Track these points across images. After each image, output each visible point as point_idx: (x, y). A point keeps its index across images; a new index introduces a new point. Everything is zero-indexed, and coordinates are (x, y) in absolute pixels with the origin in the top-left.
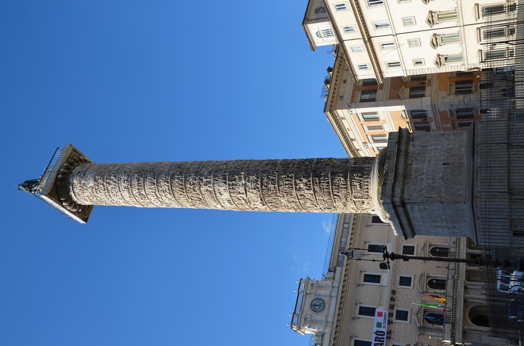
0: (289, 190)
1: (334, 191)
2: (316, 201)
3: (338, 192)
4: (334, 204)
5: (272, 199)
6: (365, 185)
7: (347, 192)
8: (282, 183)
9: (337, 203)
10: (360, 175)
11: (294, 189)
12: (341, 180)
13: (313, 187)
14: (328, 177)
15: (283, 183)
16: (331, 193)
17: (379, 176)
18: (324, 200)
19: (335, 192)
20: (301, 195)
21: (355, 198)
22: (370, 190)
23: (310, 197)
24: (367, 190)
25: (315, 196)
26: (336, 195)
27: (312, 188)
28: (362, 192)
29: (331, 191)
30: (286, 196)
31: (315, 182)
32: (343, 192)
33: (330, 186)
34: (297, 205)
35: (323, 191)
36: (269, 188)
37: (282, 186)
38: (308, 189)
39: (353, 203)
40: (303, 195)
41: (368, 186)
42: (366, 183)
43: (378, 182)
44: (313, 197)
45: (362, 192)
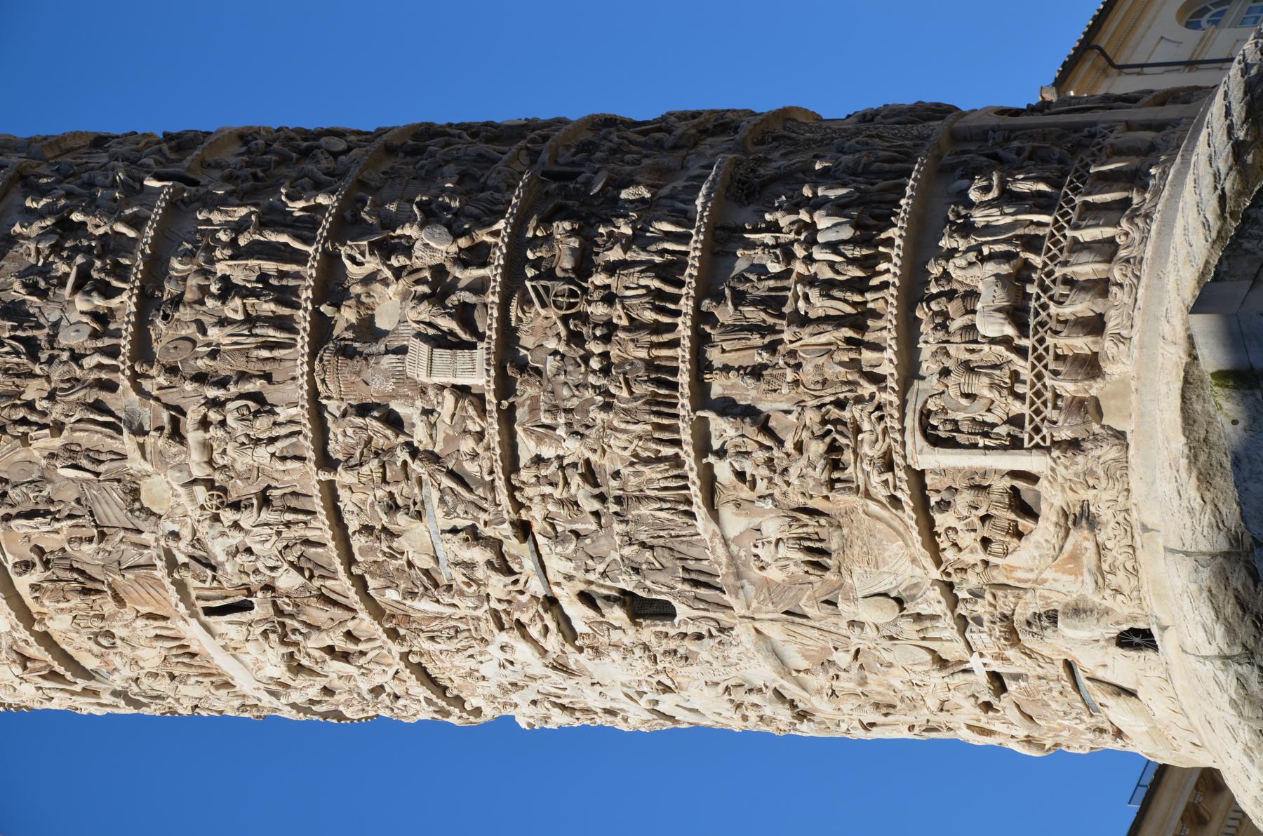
0: (246, 353)
1: (714, 356)
2: (512, 489)
3: (756, 372)
4: (703, 522)
5: (52, 456)
6: (1068, 282)
7: (854, 364)
8: (193, 281)
9: (727, 512)
10: (1042, 187)
11: (302, 340)
12: (811, 242)
13: (504, 307)
14: (684, 218)
15: (206, 273)
16: (684, 379)
17: (1241, 135)
18: (590, 475)
19: (726, 369)
20: (363, 410)
21: (936, 441)
22: (1120, 339)
23: (447, 439)
24: (1081, 344)
25: (507, 418)
26: (727, 408)
27: (488, 323)
28: (1023, 367)
29: (683, 354)
30: (204, 424)
31: (536, 264)
32: (808, 373)
33: (686, 305)
34: (307, 542)
35: (605, 355)
36: (41, 335)
37: (185, 313)
38: (442, 341)
39: (909, 514)
40: (377, 406)
41: (1105, 293)
42: (1085, 256)
43: (1222, 199)
44: (480, 436)
45: (1023, 367)
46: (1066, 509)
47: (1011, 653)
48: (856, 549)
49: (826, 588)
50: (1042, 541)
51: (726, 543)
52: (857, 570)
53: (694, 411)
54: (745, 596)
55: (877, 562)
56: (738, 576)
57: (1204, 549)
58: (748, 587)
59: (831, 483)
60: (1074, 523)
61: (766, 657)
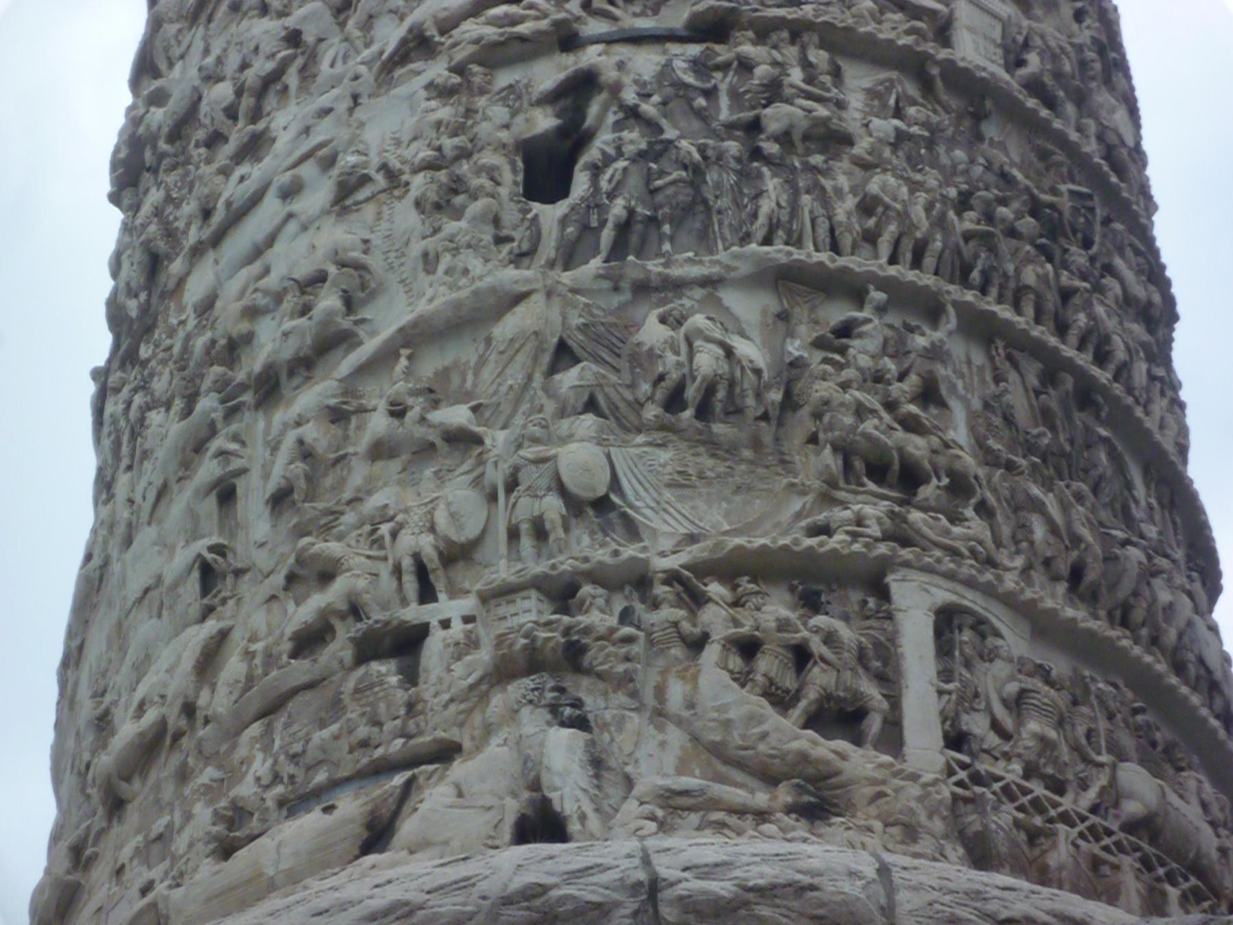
45: (1077, 802)
46: (833, 781)
47: (484, 656)
48: (710, 462)
49: (622, 405)
50: (765, 727)
51: (709, 283)
52: (664, 456)
53: (955, 304)
54: (600, 291)
55: (682, 486)
56: (643, 289)
57: (902, 896)
58: (617, 300)
59: (844, 451)
60: (798, 786)
61: (458, 305)
